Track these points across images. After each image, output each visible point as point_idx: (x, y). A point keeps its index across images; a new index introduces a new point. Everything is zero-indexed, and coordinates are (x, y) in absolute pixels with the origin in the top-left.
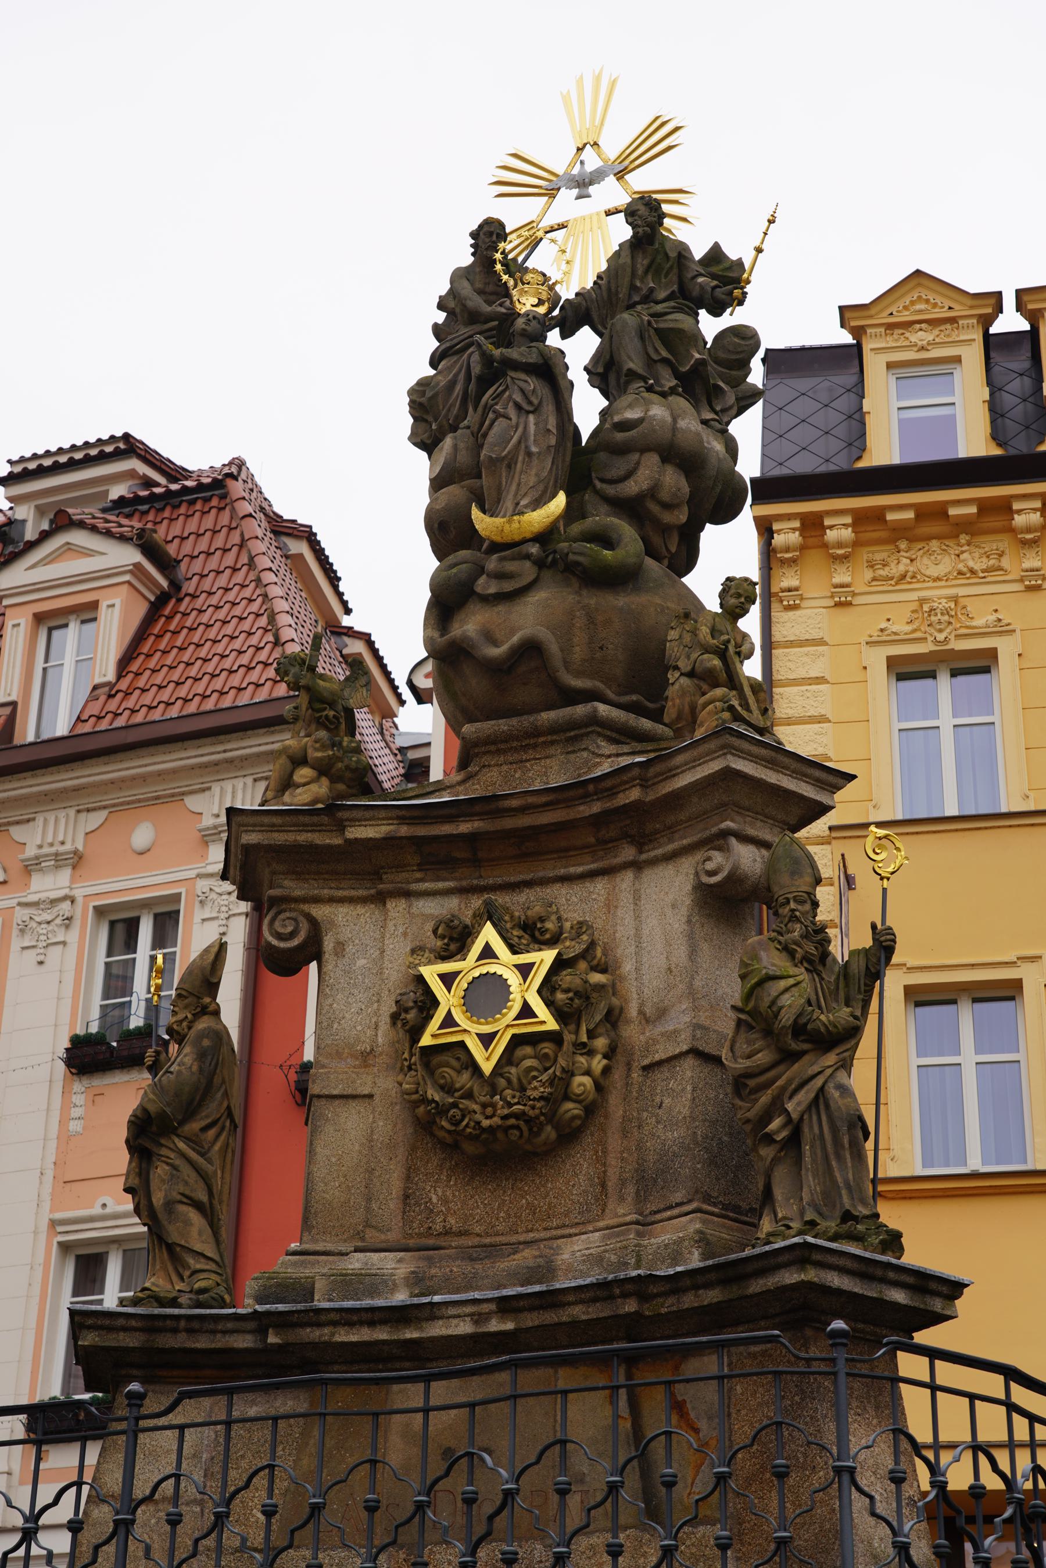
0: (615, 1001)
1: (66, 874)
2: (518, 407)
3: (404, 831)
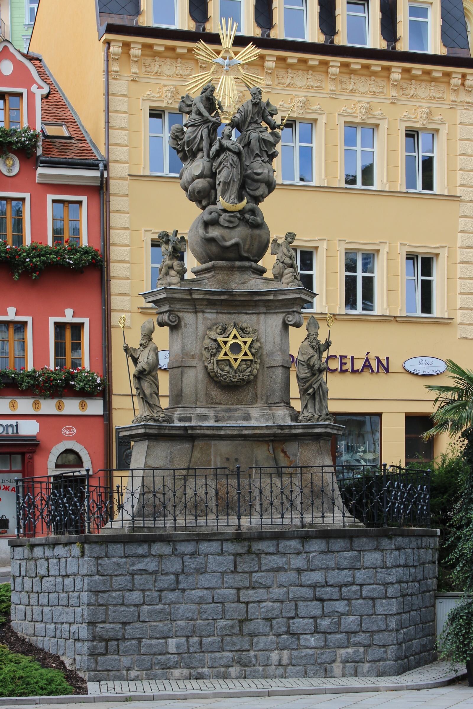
2: (231, 165)
3: (208, 297)
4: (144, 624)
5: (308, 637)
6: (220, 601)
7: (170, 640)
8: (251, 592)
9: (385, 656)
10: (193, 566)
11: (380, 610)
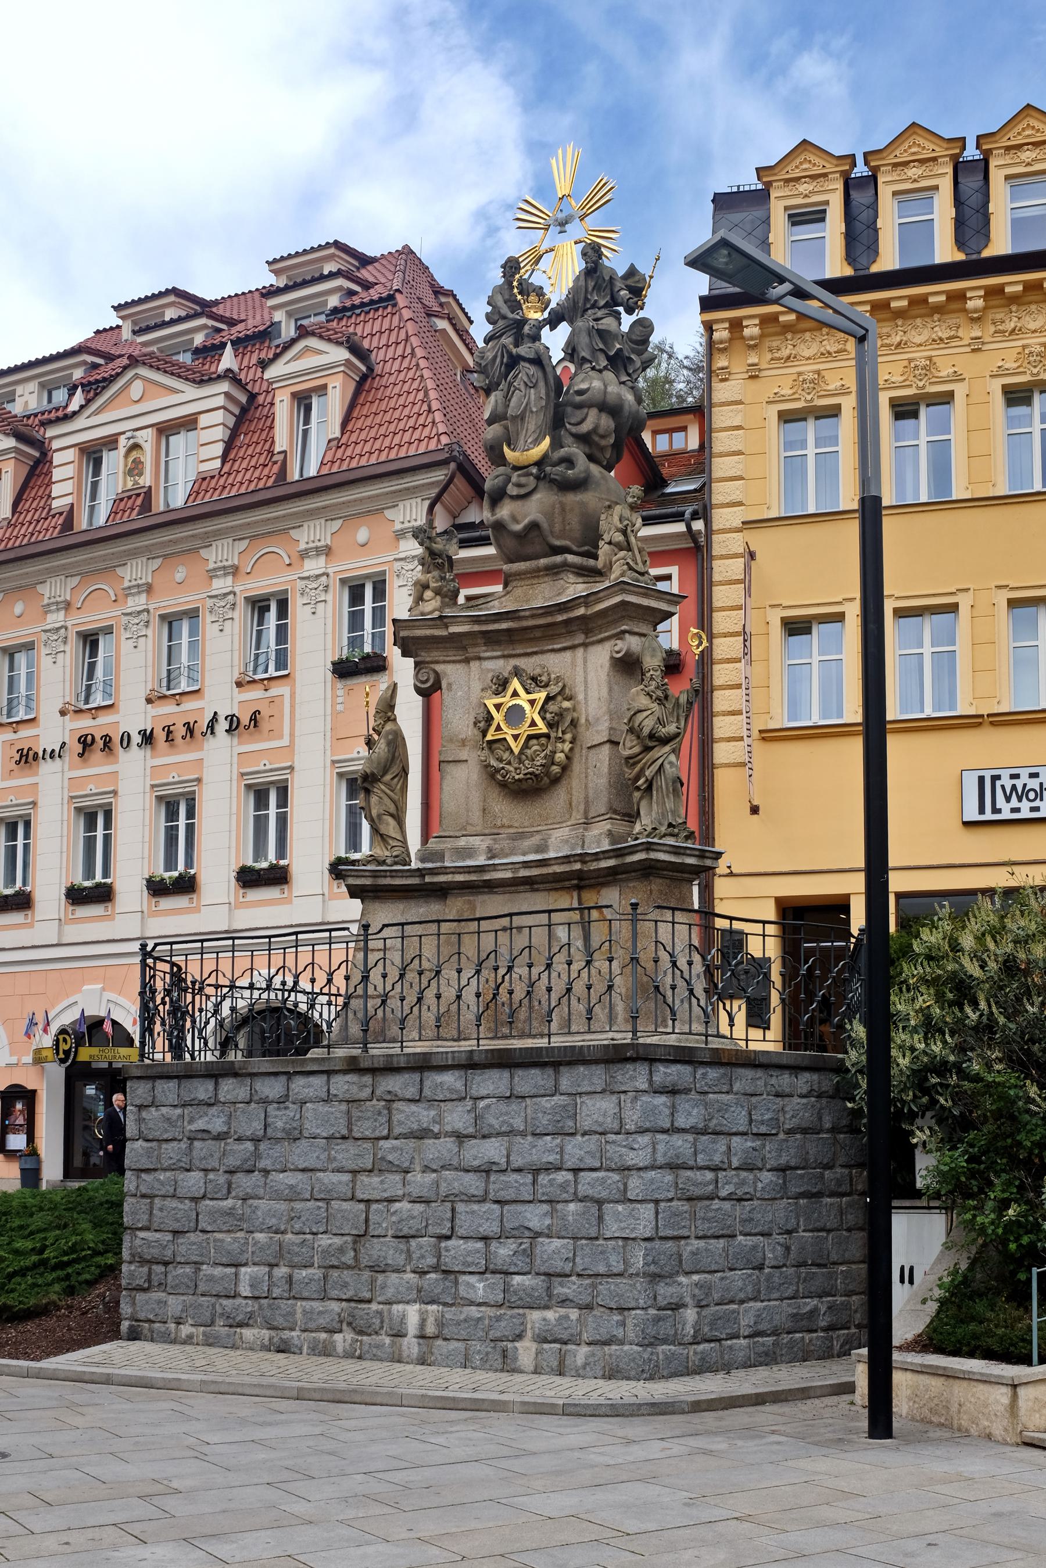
0: (575, 715)
1: (322, 559)
4: (206, 1236)
5: (472, 1279)
6: (322, 1196)
7: (243, 1270)
8: (375, 1180)
9: (619, 1333)
10: (280, 1124)
11: (612, 1228)
